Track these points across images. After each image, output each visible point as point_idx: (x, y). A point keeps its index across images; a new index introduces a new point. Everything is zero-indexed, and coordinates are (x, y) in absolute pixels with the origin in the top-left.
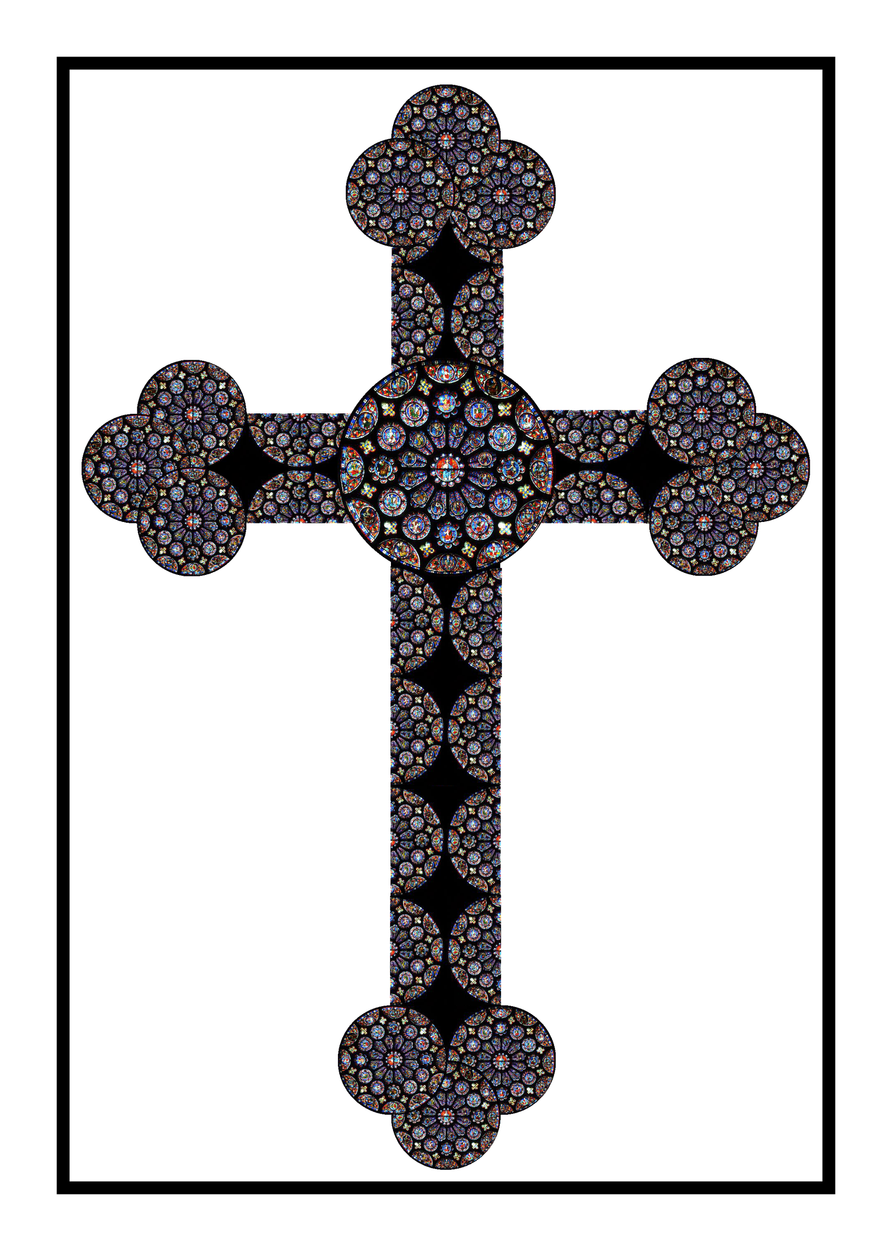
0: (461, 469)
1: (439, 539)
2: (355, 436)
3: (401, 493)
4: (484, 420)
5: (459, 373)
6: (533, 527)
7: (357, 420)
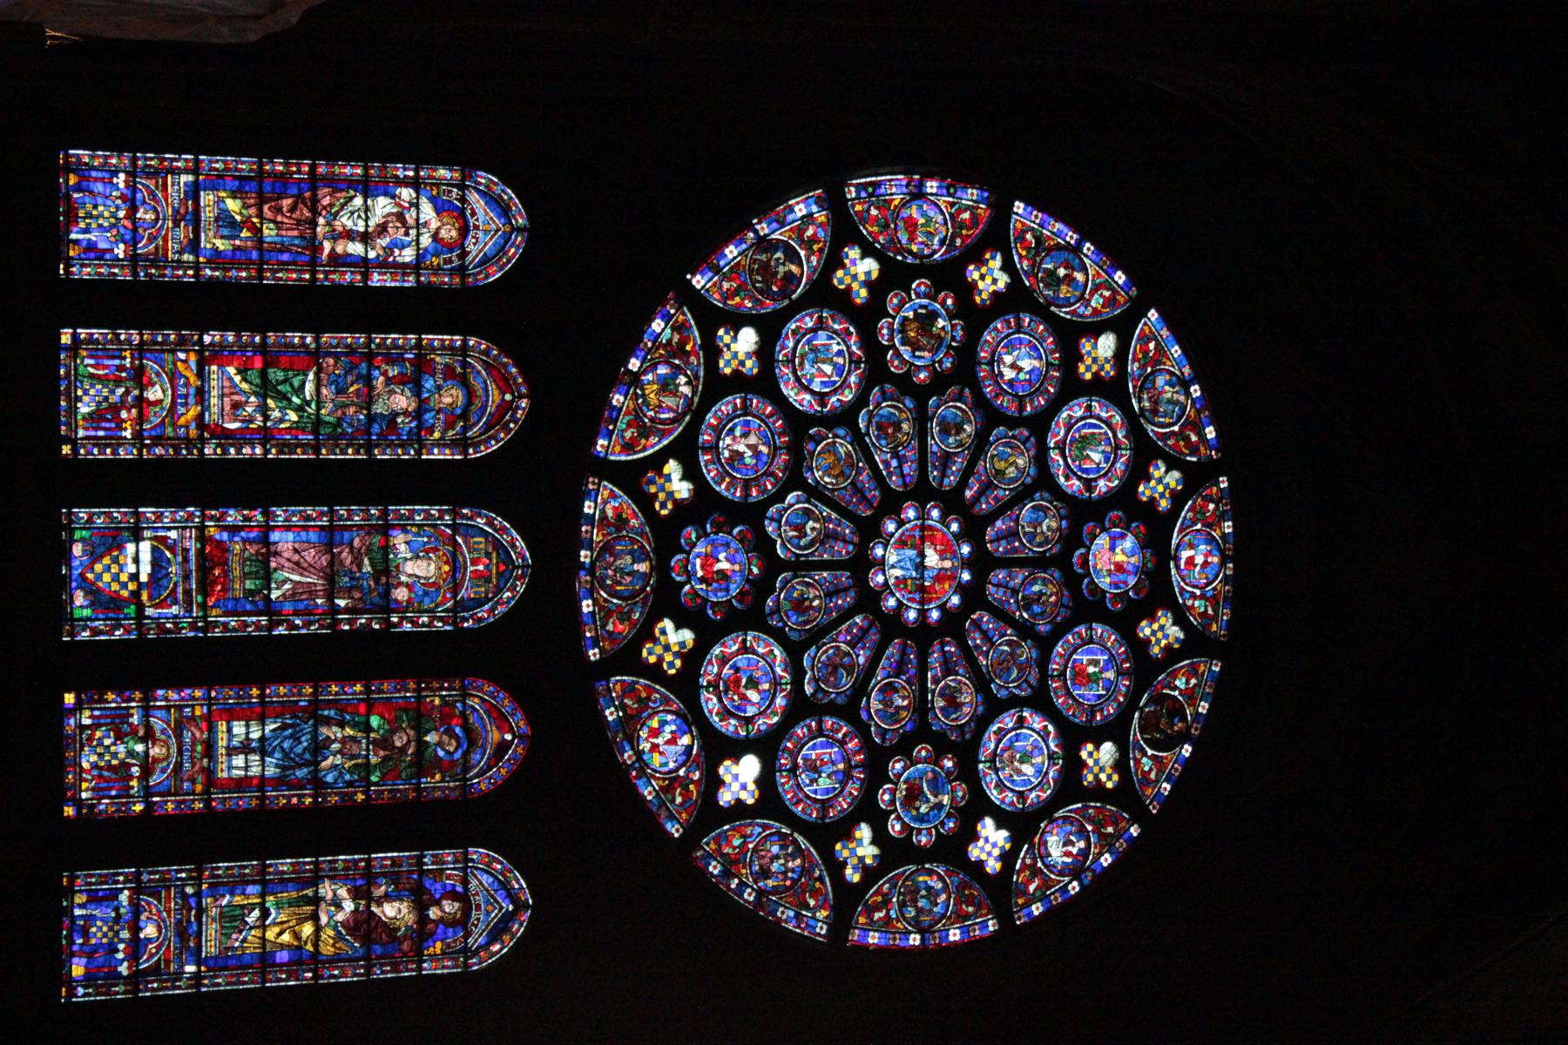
0: (923, 614)
1: (703, 534)
3: (848, 396)
4: (1069, 694)
6: (742, 885)
7: (1067, 247)
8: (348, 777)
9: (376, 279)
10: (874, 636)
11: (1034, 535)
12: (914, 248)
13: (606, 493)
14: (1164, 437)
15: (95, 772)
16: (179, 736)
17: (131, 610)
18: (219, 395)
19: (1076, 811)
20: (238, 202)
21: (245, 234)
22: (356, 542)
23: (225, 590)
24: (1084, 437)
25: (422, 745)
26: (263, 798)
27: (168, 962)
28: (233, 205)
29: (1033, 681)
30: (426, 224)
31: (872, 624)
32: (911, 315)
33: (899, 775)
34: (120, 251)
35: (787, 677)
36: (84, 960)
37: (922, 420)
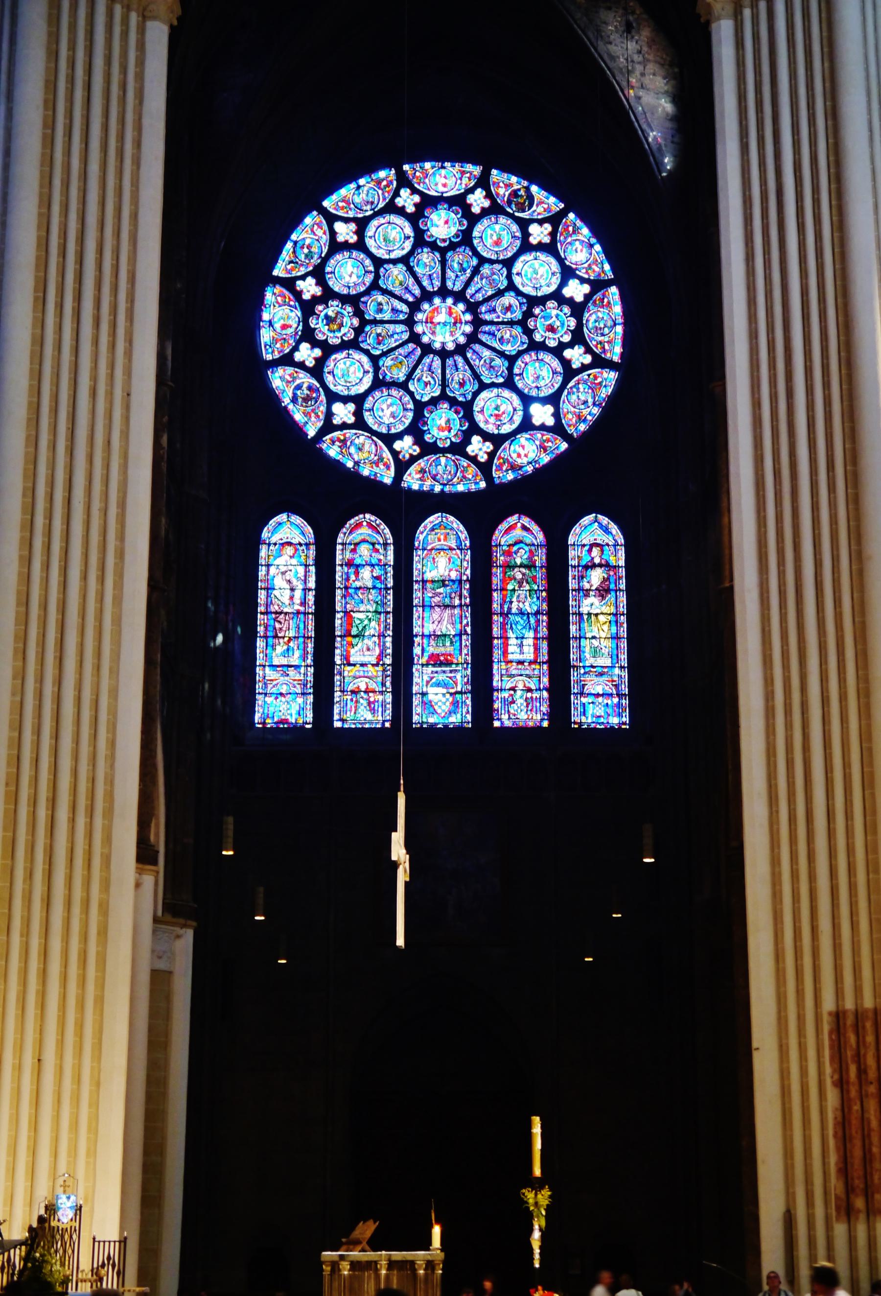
0: (466, 323)
2: (288, 272)
5: (465, 180)
8: (535, 599)
9: (312, 584)
10: (477, 347)
11: (430, 266)
12: (295, 325)
13: (409, 478)
14: (384, 199)
15: (529, 713)
16: (513, 676)
17: (458, 696)
18: (363, 659)
19: (562, 245)
20: (277, 647)
21: (291, 644)
22: (430, 595)
23: (450, 655)
24: (384, 240)
25: (521, 566)
26: (543, 638)
27: (613, 681)
28: (280, 649)
29: (501, 266)
30: (287, 561)
31: (471, 348)
32: (327, 327)
33: (542, 336)
34: (300, 700)
35: (495, 390)
36: (611, 717)
37: (375, 322)
